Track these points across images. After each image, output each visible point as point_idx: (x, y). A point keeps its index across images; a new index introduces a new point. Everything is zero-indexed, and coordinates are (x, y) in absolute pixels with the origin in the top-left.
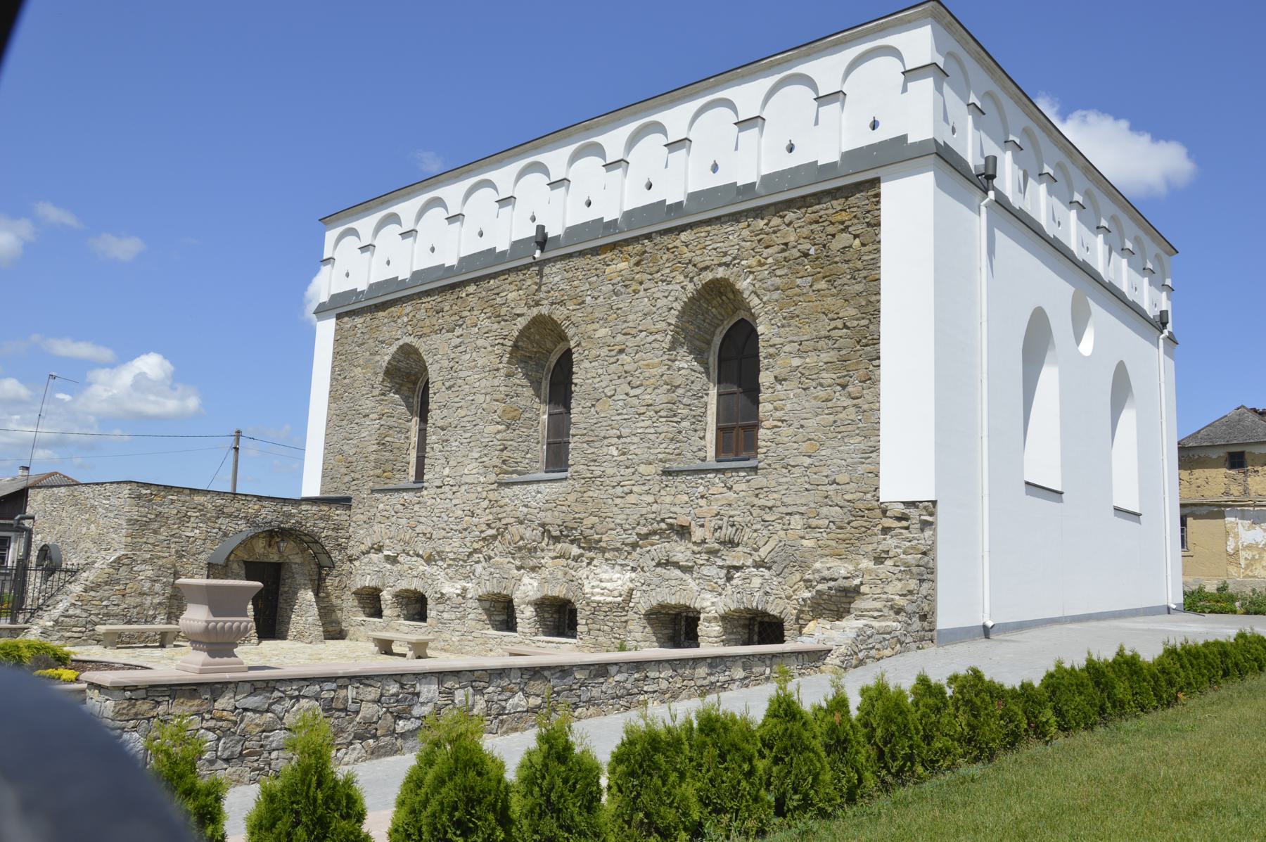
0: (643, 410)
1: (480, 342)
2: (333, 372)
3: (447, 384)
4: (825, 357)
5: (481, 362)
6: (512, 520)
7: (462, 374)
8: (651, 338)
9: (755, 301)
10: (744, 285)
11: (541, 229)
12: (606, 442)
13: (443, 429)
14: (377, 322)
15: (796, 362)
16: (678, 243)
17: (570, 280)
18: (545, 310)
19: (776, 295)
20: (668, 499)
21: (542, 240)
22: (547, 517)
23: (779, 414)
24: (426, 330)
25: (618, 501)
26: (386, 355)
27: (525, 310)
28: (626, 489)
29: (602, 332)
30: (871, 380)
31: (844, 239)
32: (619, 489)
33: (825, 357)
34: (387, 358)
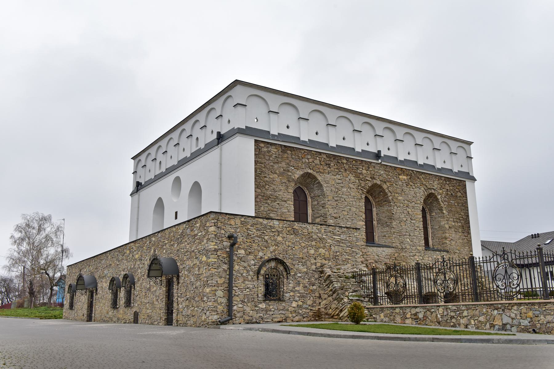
0: (416, 228)
1: (351, 186)
2: (256, 171)
3: (336, 199)
4: (460, 224)
5: (353, 194)
6: (373, 261)
7: (345, 197)
8: (416, 205)
9: (442, 203)
10: (439, 197)
11: (379, 152)
12: (405, 237)
13: (336, 218)
14: (286, 155)
15: (453, 224)
16: (421, 177)
17: (387, 175)
18: (379, 183)
19: (447, 203)
20: (427, 259)
21: (378, 155)
22: (388, 261)
23: (451, 238)
24: (321, 170)
25: (412, 257)
26: (298, 174)
27: (370, 179)
28: (414, 254)
29: (400, 198)
30: (469, 233)
31: (459, 194)
32: (412, 254)
33: (460, 224)
34: (297, 176)
